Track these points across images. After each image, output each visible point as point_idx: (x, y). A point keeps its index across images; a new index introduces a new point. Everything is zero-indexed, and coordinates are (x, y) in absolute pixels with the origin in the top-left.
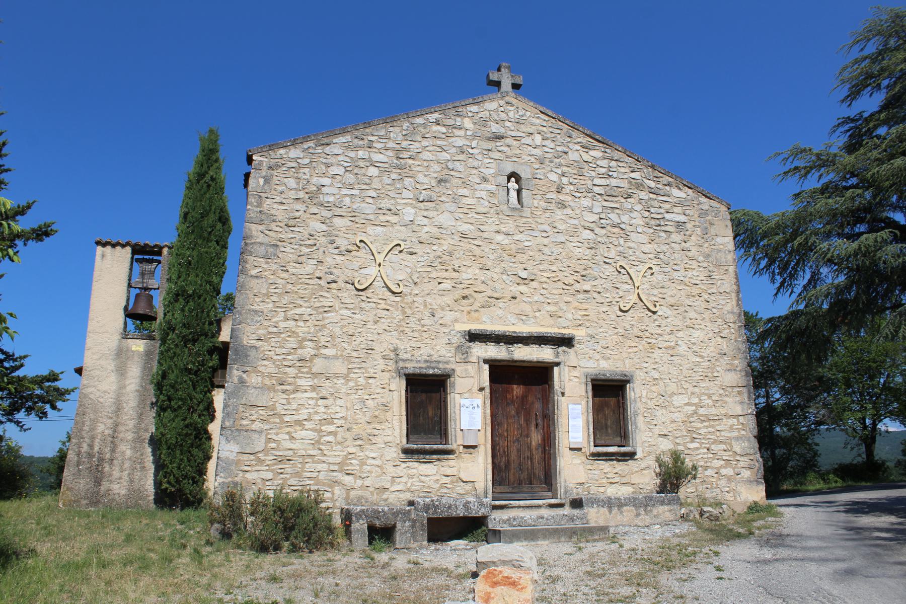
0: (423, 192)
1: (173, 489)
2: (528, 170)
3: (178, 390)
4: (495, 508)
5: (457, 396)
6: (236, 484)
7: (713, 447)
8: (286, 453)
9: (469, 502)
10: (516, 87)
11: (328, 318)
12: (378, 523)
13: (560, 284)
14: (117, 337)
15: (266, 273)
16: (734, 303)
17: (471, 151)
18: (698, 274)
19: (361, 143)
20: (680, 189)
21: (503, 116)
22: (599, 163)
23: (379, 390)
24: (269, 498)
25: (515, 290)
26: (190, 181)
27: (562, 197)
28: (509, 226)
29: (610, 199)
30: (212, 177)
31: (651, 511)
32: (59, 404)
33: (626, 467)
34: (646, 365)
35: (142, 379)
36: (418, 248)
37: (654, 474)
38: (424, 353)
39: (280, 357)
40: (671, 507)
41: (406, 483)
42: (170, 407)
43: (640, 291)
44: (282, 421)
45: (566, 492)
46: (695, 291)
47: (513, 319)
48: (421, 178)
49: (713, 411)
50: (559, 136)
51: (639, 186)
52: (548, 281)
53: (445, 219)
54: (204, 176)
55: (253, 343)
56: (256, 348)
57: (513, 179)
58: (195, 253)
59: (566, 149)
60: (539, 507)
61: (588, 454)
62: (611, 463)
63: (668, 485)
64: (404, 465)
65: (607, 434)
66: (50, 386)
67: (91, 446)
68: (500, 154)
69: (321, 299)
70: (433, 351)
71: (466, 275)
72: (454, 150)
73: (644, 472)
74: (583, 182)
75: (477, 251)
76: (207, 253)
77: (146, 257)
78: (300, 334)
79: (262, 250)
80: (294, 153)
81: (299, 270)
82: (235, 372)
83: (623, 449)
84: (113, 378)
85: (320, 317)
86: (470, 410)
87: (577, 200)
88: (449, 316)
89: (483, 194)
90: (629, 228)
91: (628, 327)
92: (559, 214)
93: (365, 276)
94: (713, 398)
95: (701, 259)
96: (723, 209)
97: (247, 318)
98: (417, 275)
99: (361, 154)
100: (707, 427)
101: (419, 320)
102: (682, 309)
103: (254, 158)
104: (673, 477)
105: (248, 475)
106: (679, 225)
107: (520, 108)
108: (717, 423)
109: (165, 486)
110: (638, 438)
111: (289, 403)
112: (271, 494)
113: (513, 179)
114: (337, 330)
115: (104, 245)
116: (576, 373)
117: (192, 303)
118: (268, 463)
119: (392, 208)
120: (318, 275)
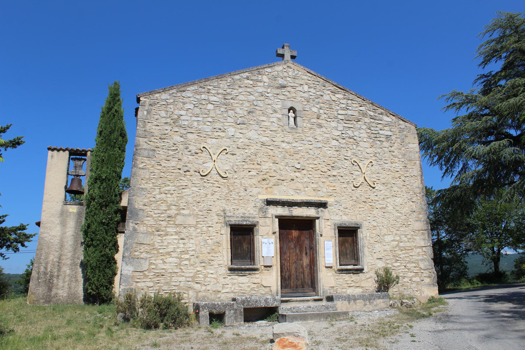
0: (240, 119)
1: (94, 293)
2: (300, 106)
3: (97, 235)
4: (283, 301)
5: (260, 237)
6: (132, 289)
7: (408, 265)
8: (161, 271)
9: (267, 299)
10: (293, 57)
11: (185, 192)
12: (215, 312)
13: (319, 172)
14: (61, 204)
15: (148, 167)
16: (420, 182)
17: (267, 95)
18: (399, 166)
19: (203, 90)
20: (388, 116)
21: (285, 74)
22: (341, 101)
23: (215, 234)
24: (151, 298)
25: (293, 175)
26: (103, 112)
27: (320, 121)
28: (289, 138)
29: (348, 122)
30: (116, 110)
31: (373, 302)
32: (26, 243)
33: (358, 277)
34: (369, 218)
35: (76, 228)
36: (237, 151)
37: (374, 281)
38: (240, 212)
39: (156, 215)
40: (384, 300)
41: (231, 288)
42: (92, 245)
43: (365, 175)
44: (159, 253)
45: (323, 292)
46: (397, 175)
47: (292, 192)
48: (238, 110)
49: (408, 244)
50: (318, 86)
51: (365, 115)
52: (312, 170)
53: (252, 134)
54: (111, 109)
55: (141, 207)
56: (143, 210)
57: (291, 111)
58: (106, 155)
59: (322, 94)
60: (308, 301)
61: (336, 270)
62: (350, 275)
63: (383, 288)
64: (229, 277)
65: (347, 258)
66: (21, 233)
67: (46, 268)
68: (284, 96)
69: (181, 181)
70: (245, 211)
71: (265, 167)
72: (257, 94)
73: (368, 280)
74: (332, 113)
75: (271, 153)
76: (113, 154)
77: (77, 157)
78: (169, 202)
79: (146, 153)
80: (164, 96)
81: (168, 164)
82: (131, 224)
83: (356, 267)
84: (58, 228)
85: (180, 191)
86: (267, 245)
87: (329, 123)
88: (255, 191)
89: (274, 120)
90: (358, 139)
91: (358, 196)
92: (318, 131)
93: (206, 168)
94: (408, 237)
95: (400, 156)
96: (413, 128)
97: (137, 193)
98: (236, 167)
99: (203, 96)
100: (404, 254)
101: (238, 193)
102: (389, 186)
103: (141, 99)
104: (385, 283)
105: (139, 284)
106: (388, 137)
107: (296, 70)
108: (410, 251)
109: (90, 291)
110: (365, 260)
111: (162, 242)
112: (152, 295)
113: (291, 111)
114: (190, 199)
115: (53, 150)
116: (329, 223)
117: (104, 184)
118: (150, 277)
119: (221, 128)
120: (178, 167)
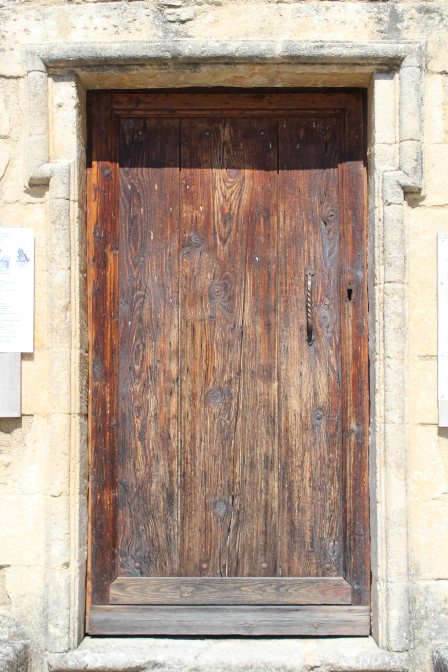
45: (413, 621)
